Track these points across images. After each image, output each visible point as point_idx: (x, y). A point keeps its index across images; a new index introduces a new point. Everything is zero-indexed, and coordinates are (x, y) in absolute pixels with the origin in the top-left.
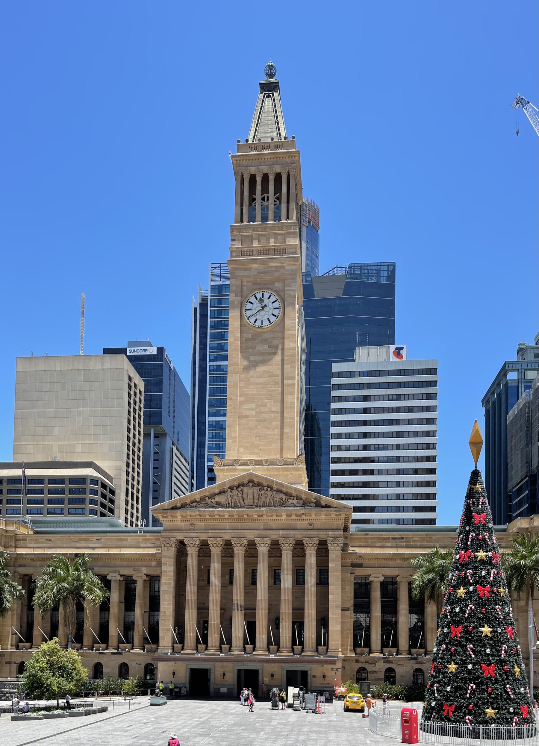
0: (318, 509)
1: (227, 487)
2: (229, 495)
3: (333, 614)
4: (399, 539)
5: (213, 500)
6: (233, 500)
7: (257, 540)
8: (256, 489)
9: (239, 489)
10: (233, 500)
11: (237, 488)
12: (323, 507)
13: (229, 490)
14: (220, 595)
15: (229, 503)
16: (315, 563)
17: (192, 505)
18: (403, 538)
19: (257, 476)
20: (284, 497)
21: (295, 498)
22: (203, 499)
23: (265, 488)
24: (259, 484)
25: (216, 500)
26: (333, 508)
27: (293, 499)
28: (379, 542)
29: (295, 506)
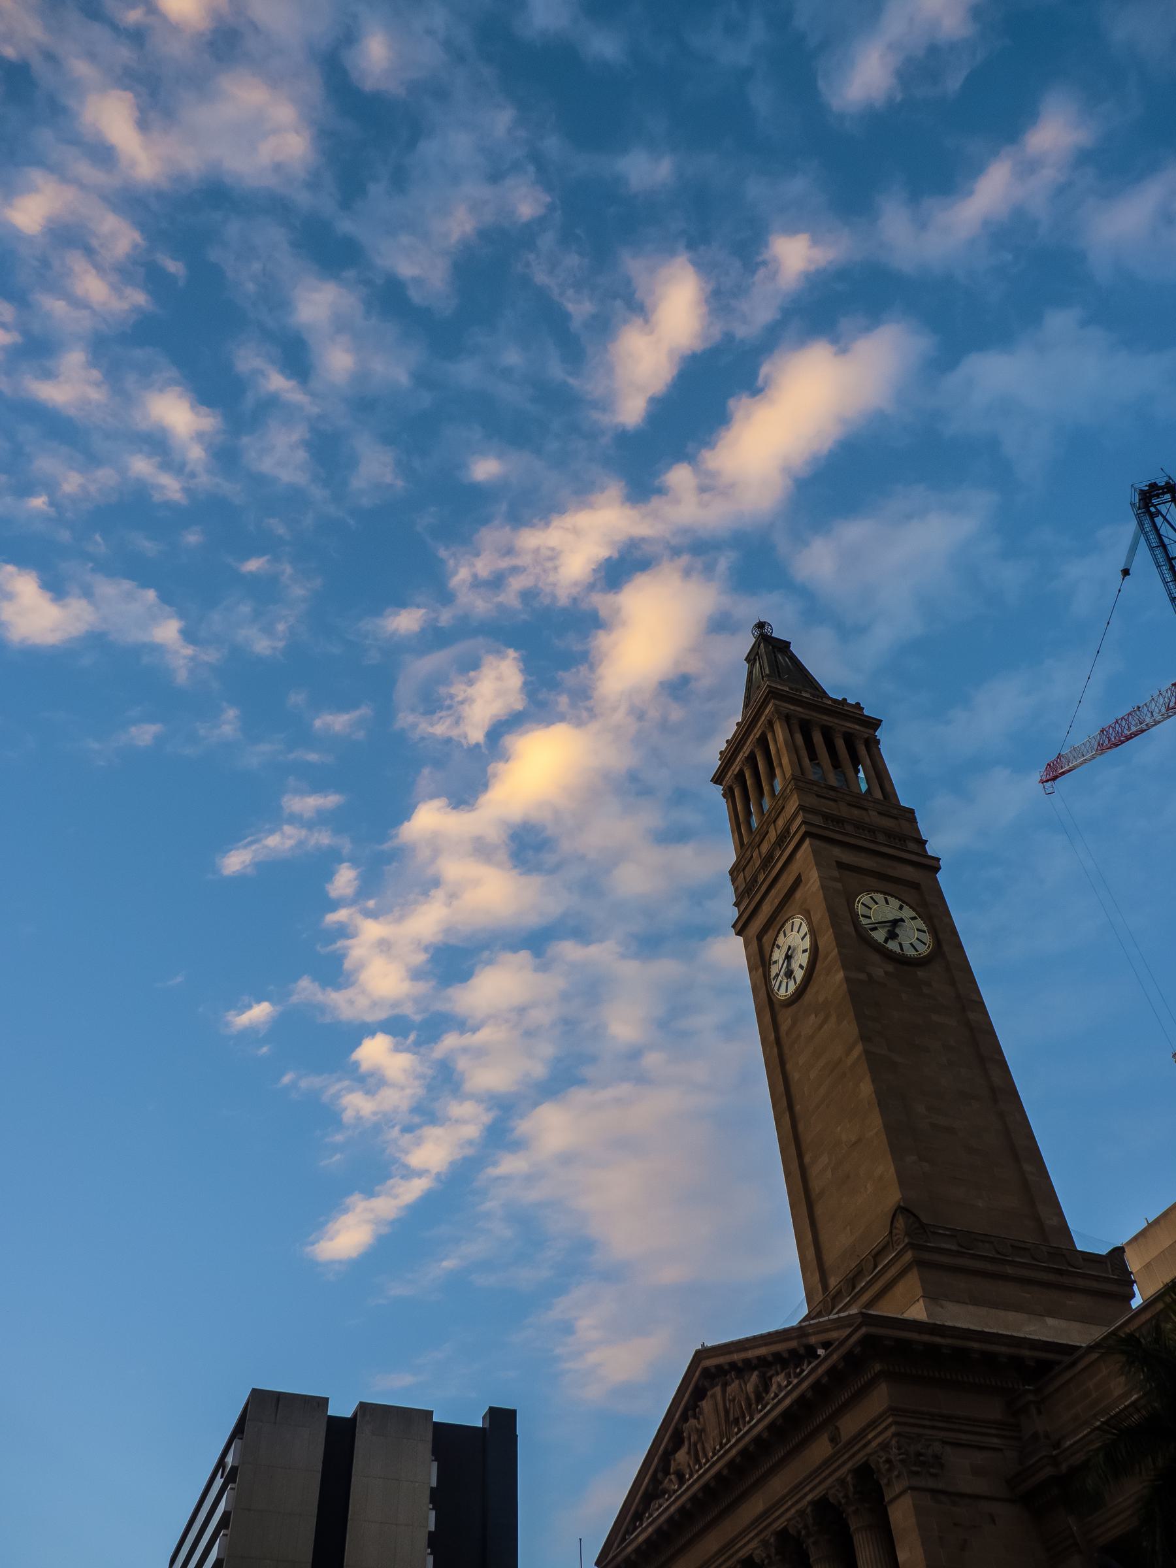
8: (718, 1390)
27: (778, 1374)
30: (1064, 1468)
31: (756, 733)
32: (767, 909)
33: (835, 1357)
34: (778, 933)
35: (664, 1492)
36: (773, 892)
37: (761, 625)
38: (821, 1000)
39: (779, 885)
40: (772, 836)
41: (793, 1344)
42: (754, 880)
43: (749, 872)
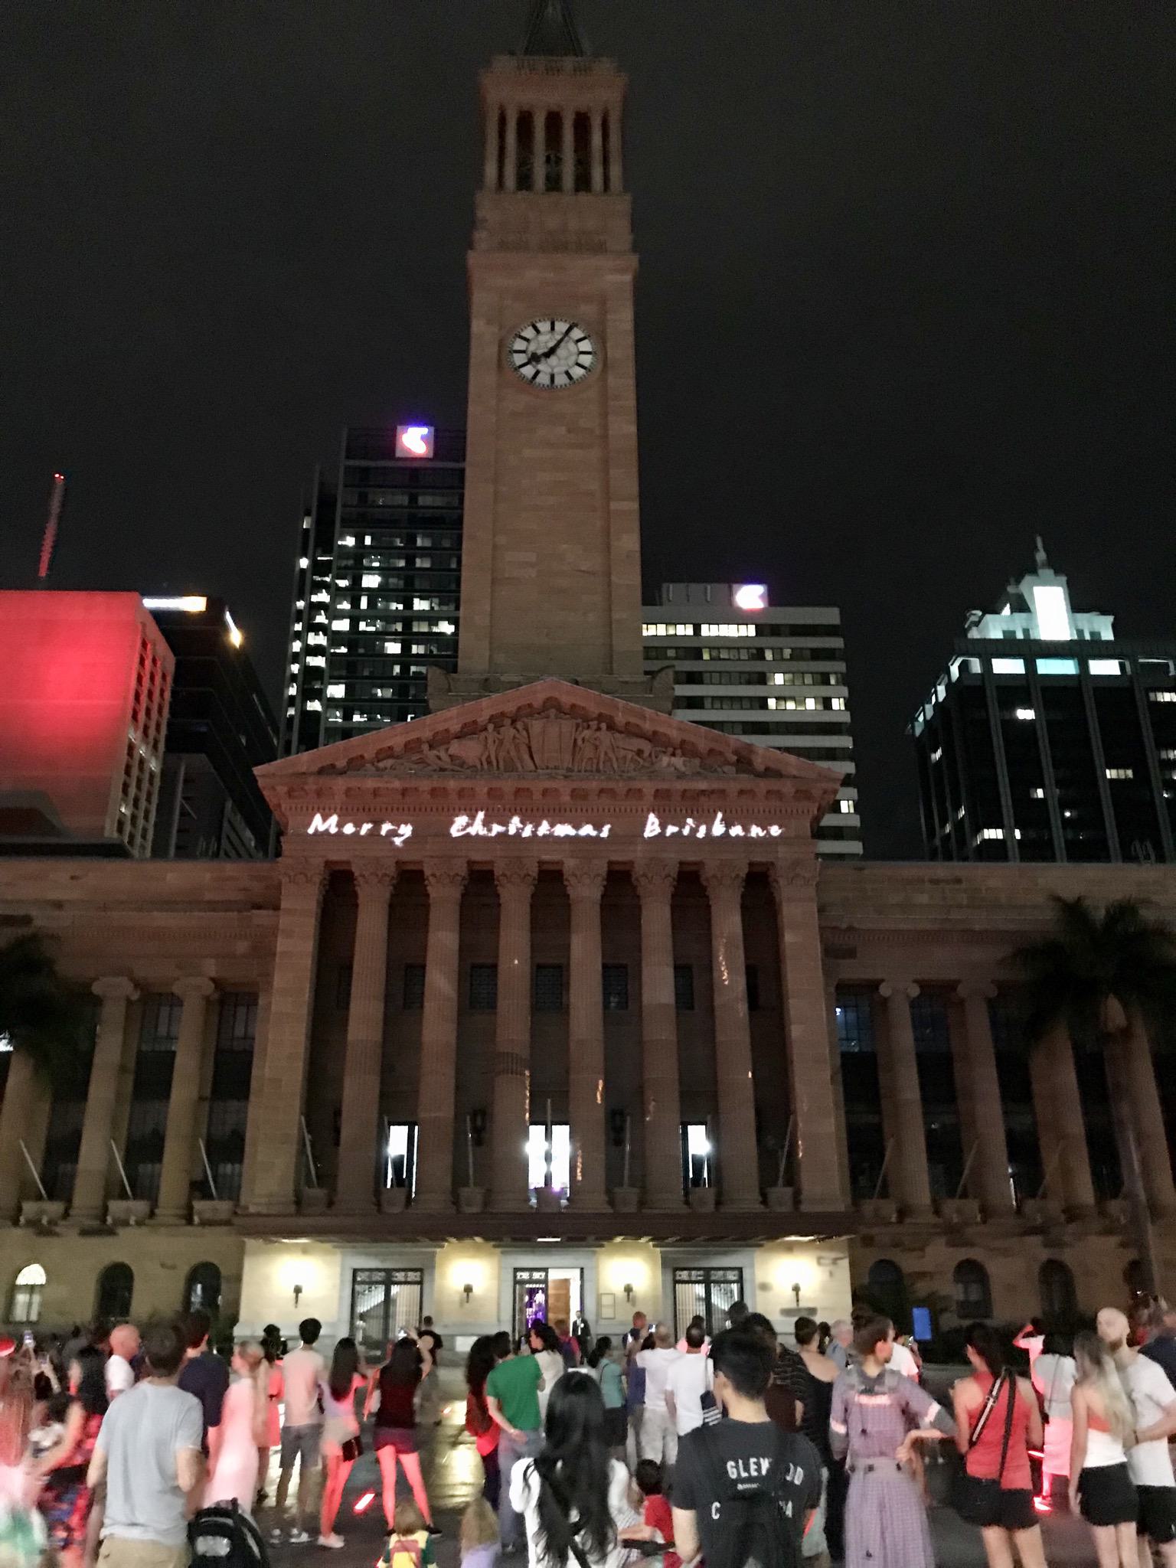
0: (746, 781)
2: (490, 741)
4: (947, 882)
8: (567, 725)
9: (519, 725)
10: (502, 754)
11: (514, 722)
12: (758, 775)
13: (491, 727)
15: (489, 763)
17: (381, 765)
18: (959, 881)
20: (646, 747)
21: (679, 752)
22: (412, 746)
23: (594, 724)
25: (452, 751)
26: (788, 777)
27: (673, 755)
29: (681, 776)
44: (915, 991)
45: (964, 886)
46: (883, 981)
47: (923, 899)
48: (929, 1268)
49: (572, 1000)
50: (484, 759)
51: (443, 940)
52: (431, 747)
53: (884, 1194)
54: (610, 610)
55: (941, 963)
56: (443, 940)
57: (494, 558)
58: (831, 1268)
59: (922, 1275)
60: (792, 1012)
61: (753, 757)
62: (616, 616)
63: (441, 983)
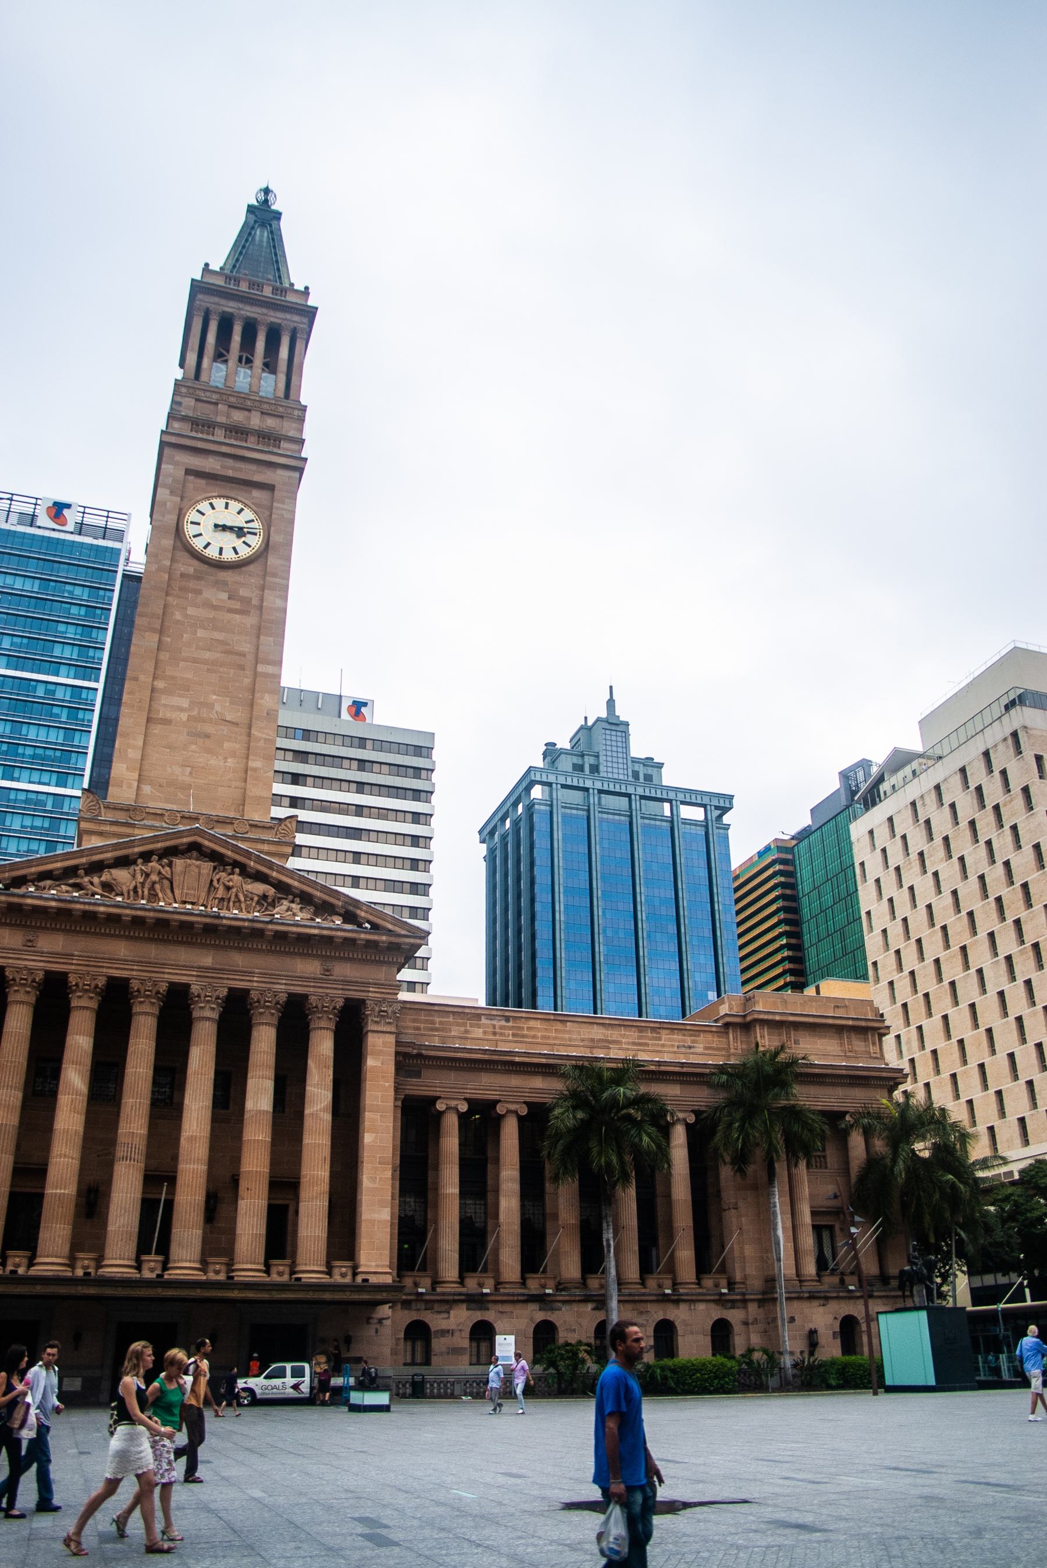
1: (137, 850)
3: (373, 1179)
5: (96, 880)
6: (147, 886)
7: (195, 989)
8: (207, 866)
9: (165, 860)
10: (147, 886)
11: (160, 859)
13: (140, 861)
14: (83, 1117)
16: (332, 1055)
17: (42, 884)
19: (213, 838)
20: (271, 891)
21: (298, 900)
24: (215, 857)
25: (103, 878)
27: (293, 902)
28: (458, 1025)
30: (415, 1051)
31: (275, 317)
32: (211, 464)
33: (384, 938)
34: (220, 497)
35: (78, 887)
36: (230, 462)
37: (267, 191)
38: (243, 592)
39: (239, 465)
40: (255, 421)
41: (340, 904)
42: (210, 426)
43: (204, 411)
44: (464, 1107)
45: (510, 1024)
46: (439, 1098)
47: (478, 1033)
48: (453, 1327)
49: (187, 1101)
50: (131, 888)
51: (80, 1042)
52: (86, 874)
53: (423, 1268)
54: (248, 758)
55: (486, 1086)
56: (80, 1042)
57: (151, 700)
58: (378, 1326)
59: (444, 1332)
60: (367, 1123)
61: (358, 912)
62: (251, 764)
63: (75, 1079)
